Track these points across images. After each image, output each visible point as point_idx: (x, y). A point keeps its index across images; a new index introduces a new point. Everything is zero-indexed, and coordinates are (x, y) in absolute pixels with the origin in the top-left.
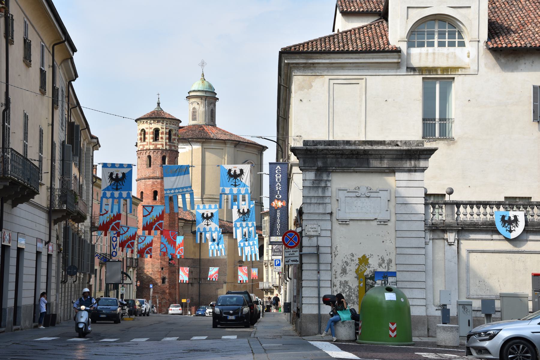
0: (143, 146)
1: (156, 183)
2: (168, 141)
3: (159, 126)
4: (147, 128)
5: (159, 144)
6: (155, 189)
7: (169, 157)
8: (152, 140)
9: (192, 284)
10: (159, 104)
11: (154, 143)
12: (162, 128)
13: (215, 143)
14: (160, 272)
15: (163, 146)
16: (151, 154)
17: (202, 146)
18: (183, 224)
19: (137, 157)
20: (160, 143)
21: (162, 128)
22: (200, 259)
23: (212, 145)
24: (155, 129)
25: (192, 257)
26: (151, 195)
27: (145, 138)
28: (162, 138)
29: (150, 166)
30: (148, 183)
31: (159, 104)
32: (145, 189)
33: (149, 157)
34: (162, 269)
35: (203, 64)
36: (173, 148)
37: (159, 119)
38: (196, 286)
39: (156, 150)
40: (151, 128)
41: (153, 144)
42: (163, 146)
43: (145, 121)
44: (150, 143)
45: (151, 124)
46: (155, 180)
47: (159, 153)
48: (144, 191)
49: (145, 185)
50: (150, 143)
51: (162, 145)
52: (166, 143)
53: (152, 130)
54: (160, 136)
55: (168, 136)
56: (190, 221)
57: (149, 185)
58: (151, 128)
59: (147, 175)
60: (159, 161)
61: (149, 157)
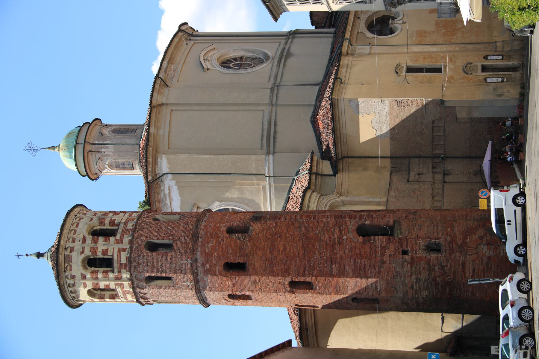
0: (125, 293)
1: (207, 266)
2: (112, 239)
3: (77, 259)
8: (111, 275)
9: (444, 175)
10: (39, 255)
11: (116, 270)
13: (157, 127)
15: (124, 250)
17: (163, 154)
18: (315, 194)
19: (155, 304)
20: (115, 257)
21: (82, 252)
22: (391, 158)
24: (85, 268)
25: (387, 175)
27: (107, 289)
28: (105, 252)
29: (169, 278)
31: (39, 255)
32: (221, 289)
35: (32, 149)
36: (130, 226)
37: (61, 258)
38: (449, 165)
42: (124, 250)
43: (68, 290)
45: (73, 277)
46: (200, 269)
49: (213, 289)
51: (121, 250)
52: (117, 242)
55: (101, 239)
56: (310, 179)
61: (150, 279)
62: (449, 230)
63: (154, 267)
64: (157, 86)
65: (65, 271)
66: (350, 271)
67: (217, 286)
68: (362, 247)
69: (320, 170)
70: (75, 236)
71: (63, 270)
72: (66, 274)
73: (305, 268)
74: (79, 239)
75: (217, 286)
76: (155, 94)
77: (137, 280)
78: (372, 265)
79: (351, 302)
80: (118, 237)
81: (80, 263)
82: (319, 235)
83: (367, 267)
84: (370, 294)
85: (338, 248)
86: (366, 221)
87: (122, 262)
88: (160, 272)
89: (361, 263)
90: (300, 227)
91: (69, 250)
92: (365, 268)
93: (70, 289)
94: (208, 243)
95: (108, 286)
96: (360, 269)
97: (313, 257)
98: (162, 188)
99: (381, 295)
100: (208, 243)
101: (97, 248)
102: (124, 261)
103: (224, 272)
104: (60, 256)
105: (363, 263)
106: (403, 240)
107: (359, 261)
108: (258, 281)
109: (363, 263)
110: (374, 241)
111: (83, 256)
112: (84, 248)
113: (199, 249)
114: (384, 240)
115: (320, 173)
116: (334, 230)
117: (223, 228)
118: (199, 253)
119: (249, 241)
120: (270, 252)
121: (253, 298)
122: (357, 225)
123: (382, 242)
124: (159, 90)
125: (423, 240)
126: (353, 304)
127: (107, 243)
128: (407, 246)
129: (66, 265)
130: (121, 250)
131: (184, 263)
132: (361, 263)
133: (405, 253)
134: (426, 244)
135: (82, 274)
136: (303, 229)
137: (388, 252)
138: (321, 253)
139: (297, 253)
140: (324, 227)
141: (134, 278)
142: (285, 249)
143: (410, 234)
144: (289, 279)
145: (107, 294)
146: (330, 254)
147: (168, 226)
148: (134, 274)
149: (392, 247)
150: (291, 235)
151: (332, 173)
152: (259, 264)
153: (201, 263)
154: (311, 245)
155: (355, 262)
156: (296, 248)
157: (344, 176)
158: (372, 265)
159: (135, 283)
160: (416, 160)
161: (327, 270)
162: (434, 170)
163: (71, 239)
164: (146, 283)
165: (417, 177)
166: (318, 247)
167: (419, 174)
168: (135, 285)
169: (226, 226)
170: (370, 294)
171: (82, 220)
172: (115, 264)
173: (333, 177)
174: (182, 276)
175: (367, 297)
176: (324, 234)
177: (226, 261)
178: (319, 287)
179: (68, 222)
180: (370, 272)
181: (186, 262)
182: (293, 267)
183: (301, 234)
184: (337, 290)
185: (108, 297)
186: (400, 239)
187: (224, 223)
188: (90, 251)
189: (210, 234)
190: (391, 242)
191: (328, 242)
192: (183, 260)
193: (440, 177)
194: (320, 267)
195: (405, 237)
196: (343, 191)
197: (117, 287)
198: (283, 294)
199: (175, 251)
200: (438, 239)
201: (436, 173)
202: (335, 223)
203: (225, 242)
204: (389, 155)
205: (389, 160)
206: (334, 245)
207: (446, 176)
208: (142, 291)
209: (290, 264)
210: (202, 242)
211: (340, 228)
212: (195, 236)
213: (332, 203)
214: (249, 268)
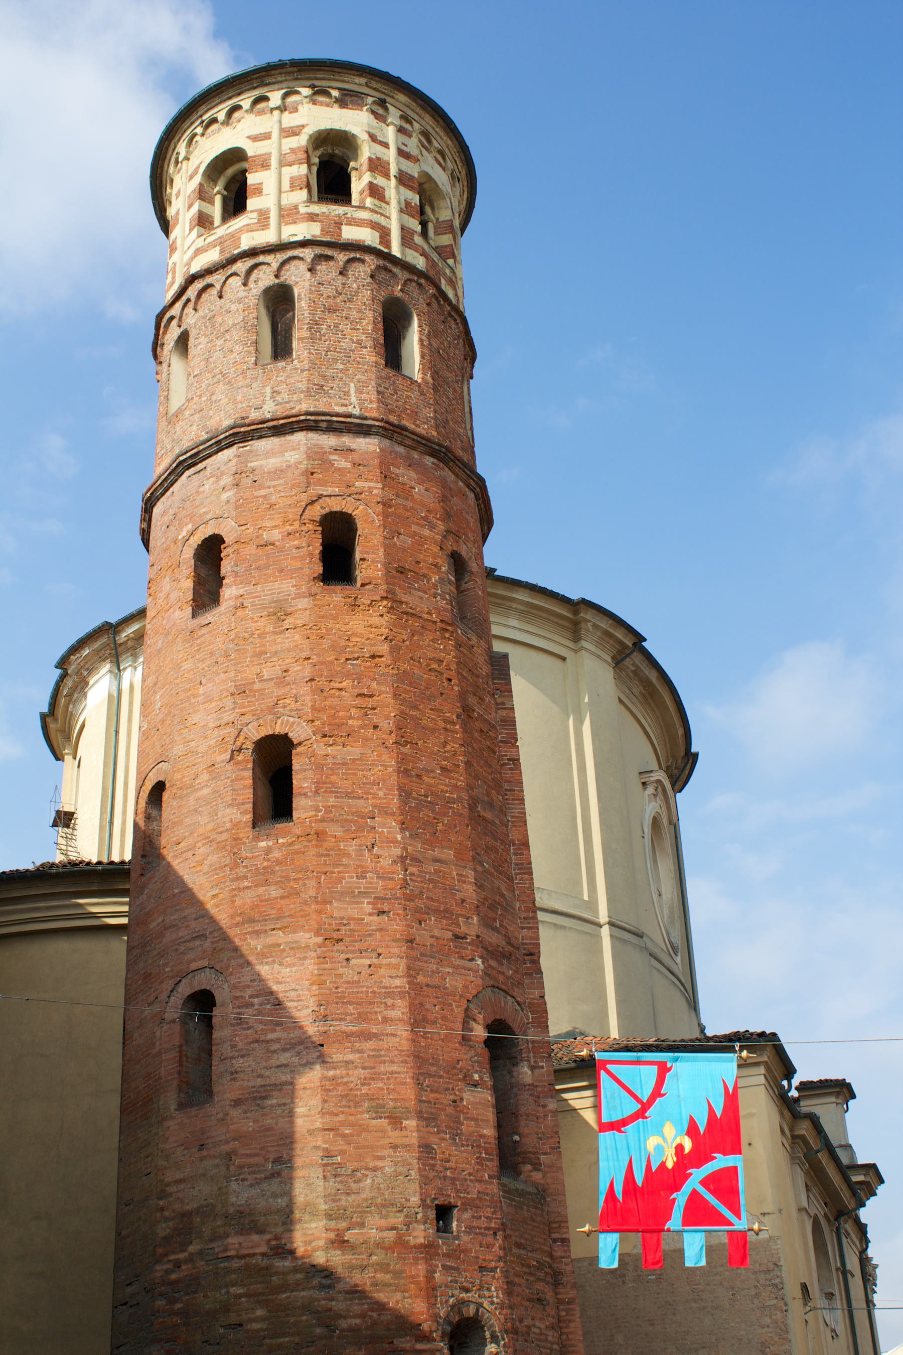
4: (255, 138)
5: (353, 222)
6: (336, 505)
7: (431, 336)
11: (317, 209)
12: (373, 138)
13: (530, 613)
14: (428, 1250)
16: (298, 278)
23: (513, 622)
26: (307, 552)
28: (375, 191)
30: (272, 463)
33: (279, 300)
34: (443, 1213)
37: (357, 83)
39: (327, 248)
40: (293, 132)
41: (312, 217)
44: (288, 215)
46: (329, 441)
47: (362, 271)
48: (228, 530)
50: (288, 215)
53: (302, 140)
54: (358, 184)
57: (278, 473)
58: (293, 132)
59: (269, 409)
60: (365, 323)
61: (279, 300)
63: (332, 310)
64: (619, 634)
65: (312, 87)
66: (349, 974)
67: (263, 492)
71: (317, 83)
72: (306, 91)
73: (347, 795)
74: (409, 145)
75: (263, 492)
76: (604, 624)
77: (283, 264)
78: (382, 1068)
79: (186, 989)
80: (418, 240)
81: (337, 126)
83: (371, 1044)
84: (239, 1063)
86: (532, 1068)
87: (344, 228)
88: (314, 324)
89: (386, 1020)
90: (490, 805)
91: (380, 111)
92: (367, 1036)
93: (246, 104)
95: (259, 191)
96: (362, 1017)
99: (235, 1113)
101: (387, 176)
102: (349, 233)
103: (317, 511)
104: (363, 81)
105: (390, 1029)
107: (396, 1014)
108: (289, 622)
109: (390, 1029)
111: (363, 137)
113: (401, 449)
121: (210, 616)
124: (610, 635)
126: (177, 1000)
127: (403, 206)
129: (335, 93)
131: (347, 394)
132: (386, 1020)
135: (303, 126)
136: (488, 815)
138: (417, 860)
141: (290, 253)
144: (298, 731)
145: (216, 210)
147: (455, 390)
148: (308, 253)
152: (361, 630)
153: (353, 446)
155: (389, 995)
158: (382, 1068)
159: (268, 258)
161: (350, 879)
164: (267, 291)
166: (437, 853)
168: (261, 259)
170: (239, 1063)
172: (338, 210)
174: (303, 386)
175: (226, 1050)
177: (360, 525)
178: (268, 850)
179: (449, 142)
180: (350, 1057)
181: (353, 399)
182: (353, 751)
184: (252, 921)
185: (205, 211)
188: (378, 159)
192: (359, 391)
194: (359, 853)
197: (255, 215)
198: (227, 717)
202: (513, 941)
208: (236, 282)
209: (366, 739)
211: (503, 955)
214: (337, 595)
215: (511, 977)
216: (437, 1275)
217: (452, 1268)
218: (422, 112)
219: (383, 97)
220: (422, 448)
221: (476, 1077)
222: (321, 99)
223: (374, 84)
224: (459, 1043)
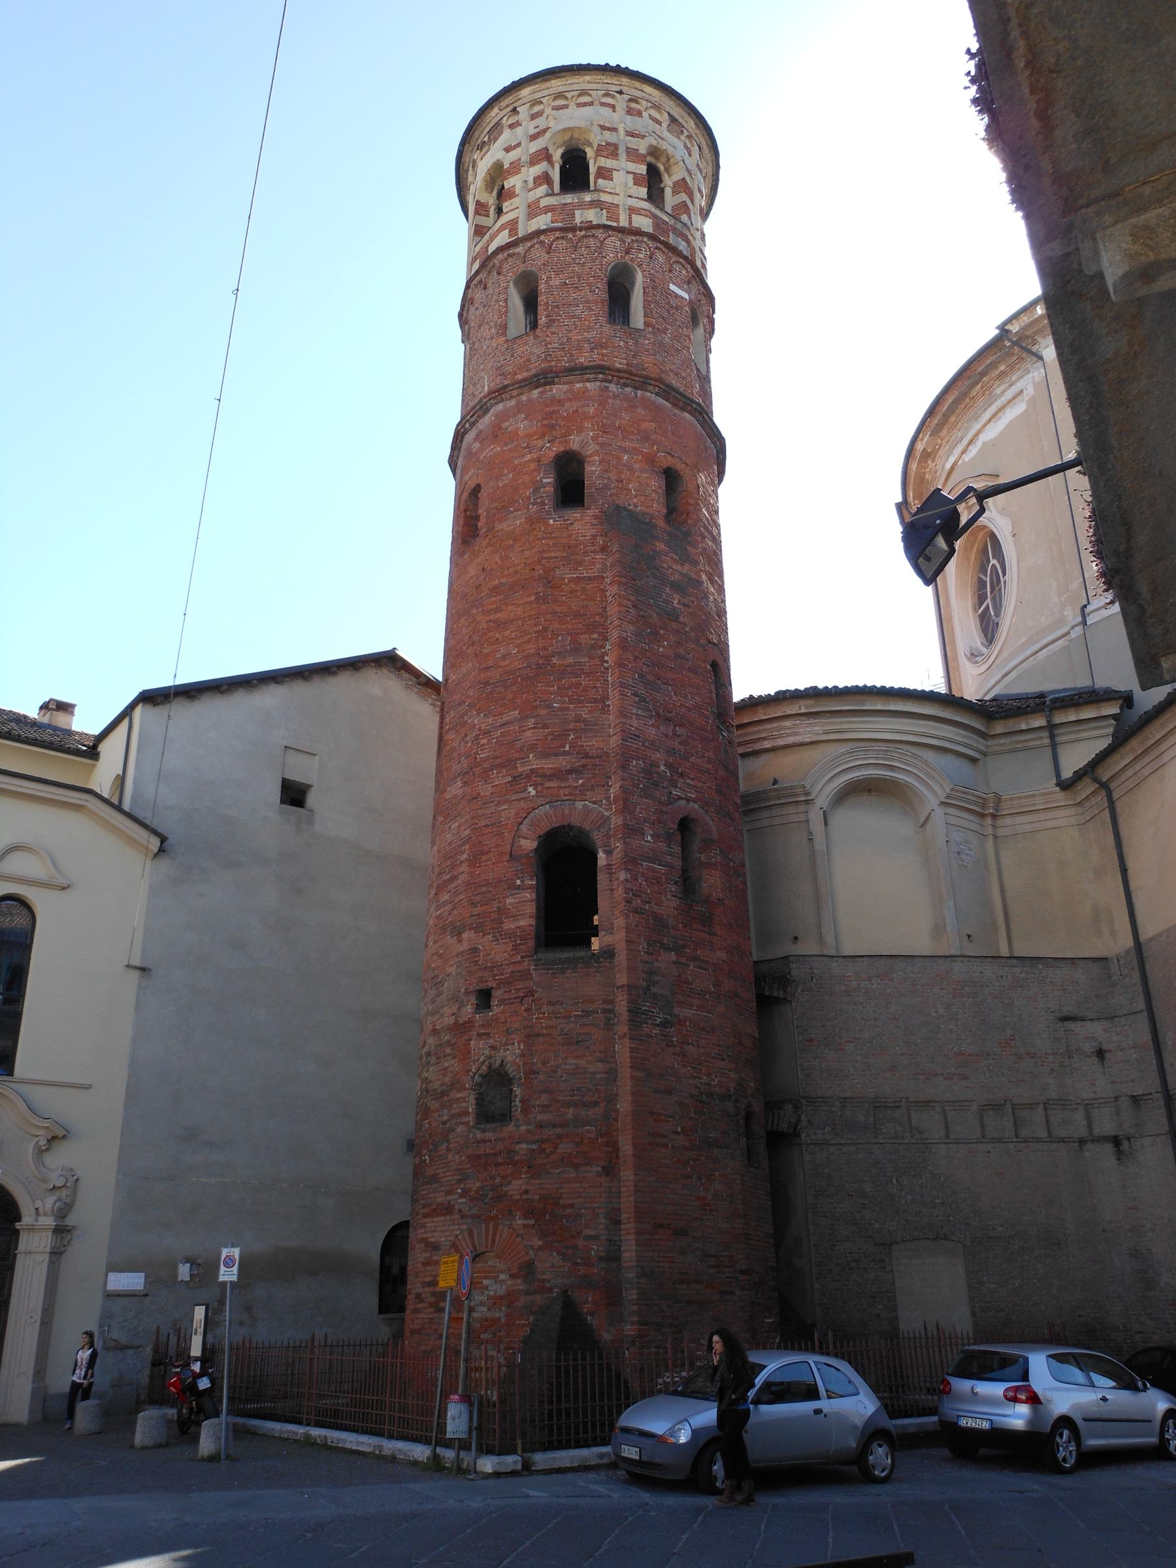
9: (1116, 1141)
21: (508, 150)
62: (565, 1148)
68: (501, 854)
69: (1073, 736)
70: (548, 111)
82: (543, 712)
85: (500, 778)
90: (576, 649)
94: (526, 418)
97: (479, 711)
98: (1014, 379)
100: (526, 418)
104: (496, 110)
106: (520, 985)
107: (465, 856)
109: (462, 869)
110: (518, 887)
112: (519, 145)
113: (513, 402)
114: (522, 923)
115: (1058, 739)
116: (565, 753)
117: (575, 442)
118: (500, 406)
119: (530, 520)
120: (496, 587)
122: (587, 826)
123: (515, 917)
125: (522, 1055)
128: (502, 1002)
130: (513, 225)
133: (484, 998)
134: (511, 1070)
136: (570, 660)
137: (485, 942)
139: (490, 663)
140: (578, 719)
142: (500, 625)
143: (545, 1008)
146: (484, 760)
149: (498, 952)
150: (545, 629)
151: (1067, 774)
154: (510, 696)
156: (504, 657)
157: (1062, 813)
158: (457, 899)
160: (1147, 1037)
162: (1125, 1103)
163: (536, 109)
165: (1089, 1047)
166: (505, 718)
167: (1100, 1053)
169: (584, 444)
171: (608, 110)
173: (1054, 781)
176: (545, 726)
179: (588, 78)
183: (548, 658)
186: (526, 975)
187: (594, 438)
189: (554, 412)
190: (515, 947)
191: (519, 744)
193: (1106, 1125)
195: (531, 993)
196: (1008, 821)
199: (507, 349)
200: (526, 1110)
201: (1118, 1113)
203: (528, 457)
204: (1143, 937)
205: (1129, 943)
206: (509, 764)
207: (1109, 1147)
210: (530, 401)
211: (569, 772)
212: (544, 379)
213: (907, 785)
215: (582, 785)
216: (472, 1043)
217: (485, 1034)
218: (548, 84)
219: (511, 108)
220: (526, 389)
221: (518, 882)
222: (484, 150)
223: (503, 104)
224: (508, 861)
